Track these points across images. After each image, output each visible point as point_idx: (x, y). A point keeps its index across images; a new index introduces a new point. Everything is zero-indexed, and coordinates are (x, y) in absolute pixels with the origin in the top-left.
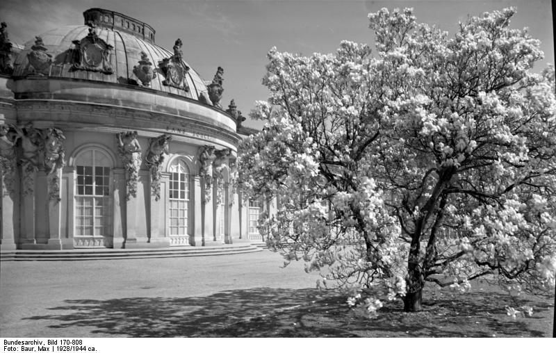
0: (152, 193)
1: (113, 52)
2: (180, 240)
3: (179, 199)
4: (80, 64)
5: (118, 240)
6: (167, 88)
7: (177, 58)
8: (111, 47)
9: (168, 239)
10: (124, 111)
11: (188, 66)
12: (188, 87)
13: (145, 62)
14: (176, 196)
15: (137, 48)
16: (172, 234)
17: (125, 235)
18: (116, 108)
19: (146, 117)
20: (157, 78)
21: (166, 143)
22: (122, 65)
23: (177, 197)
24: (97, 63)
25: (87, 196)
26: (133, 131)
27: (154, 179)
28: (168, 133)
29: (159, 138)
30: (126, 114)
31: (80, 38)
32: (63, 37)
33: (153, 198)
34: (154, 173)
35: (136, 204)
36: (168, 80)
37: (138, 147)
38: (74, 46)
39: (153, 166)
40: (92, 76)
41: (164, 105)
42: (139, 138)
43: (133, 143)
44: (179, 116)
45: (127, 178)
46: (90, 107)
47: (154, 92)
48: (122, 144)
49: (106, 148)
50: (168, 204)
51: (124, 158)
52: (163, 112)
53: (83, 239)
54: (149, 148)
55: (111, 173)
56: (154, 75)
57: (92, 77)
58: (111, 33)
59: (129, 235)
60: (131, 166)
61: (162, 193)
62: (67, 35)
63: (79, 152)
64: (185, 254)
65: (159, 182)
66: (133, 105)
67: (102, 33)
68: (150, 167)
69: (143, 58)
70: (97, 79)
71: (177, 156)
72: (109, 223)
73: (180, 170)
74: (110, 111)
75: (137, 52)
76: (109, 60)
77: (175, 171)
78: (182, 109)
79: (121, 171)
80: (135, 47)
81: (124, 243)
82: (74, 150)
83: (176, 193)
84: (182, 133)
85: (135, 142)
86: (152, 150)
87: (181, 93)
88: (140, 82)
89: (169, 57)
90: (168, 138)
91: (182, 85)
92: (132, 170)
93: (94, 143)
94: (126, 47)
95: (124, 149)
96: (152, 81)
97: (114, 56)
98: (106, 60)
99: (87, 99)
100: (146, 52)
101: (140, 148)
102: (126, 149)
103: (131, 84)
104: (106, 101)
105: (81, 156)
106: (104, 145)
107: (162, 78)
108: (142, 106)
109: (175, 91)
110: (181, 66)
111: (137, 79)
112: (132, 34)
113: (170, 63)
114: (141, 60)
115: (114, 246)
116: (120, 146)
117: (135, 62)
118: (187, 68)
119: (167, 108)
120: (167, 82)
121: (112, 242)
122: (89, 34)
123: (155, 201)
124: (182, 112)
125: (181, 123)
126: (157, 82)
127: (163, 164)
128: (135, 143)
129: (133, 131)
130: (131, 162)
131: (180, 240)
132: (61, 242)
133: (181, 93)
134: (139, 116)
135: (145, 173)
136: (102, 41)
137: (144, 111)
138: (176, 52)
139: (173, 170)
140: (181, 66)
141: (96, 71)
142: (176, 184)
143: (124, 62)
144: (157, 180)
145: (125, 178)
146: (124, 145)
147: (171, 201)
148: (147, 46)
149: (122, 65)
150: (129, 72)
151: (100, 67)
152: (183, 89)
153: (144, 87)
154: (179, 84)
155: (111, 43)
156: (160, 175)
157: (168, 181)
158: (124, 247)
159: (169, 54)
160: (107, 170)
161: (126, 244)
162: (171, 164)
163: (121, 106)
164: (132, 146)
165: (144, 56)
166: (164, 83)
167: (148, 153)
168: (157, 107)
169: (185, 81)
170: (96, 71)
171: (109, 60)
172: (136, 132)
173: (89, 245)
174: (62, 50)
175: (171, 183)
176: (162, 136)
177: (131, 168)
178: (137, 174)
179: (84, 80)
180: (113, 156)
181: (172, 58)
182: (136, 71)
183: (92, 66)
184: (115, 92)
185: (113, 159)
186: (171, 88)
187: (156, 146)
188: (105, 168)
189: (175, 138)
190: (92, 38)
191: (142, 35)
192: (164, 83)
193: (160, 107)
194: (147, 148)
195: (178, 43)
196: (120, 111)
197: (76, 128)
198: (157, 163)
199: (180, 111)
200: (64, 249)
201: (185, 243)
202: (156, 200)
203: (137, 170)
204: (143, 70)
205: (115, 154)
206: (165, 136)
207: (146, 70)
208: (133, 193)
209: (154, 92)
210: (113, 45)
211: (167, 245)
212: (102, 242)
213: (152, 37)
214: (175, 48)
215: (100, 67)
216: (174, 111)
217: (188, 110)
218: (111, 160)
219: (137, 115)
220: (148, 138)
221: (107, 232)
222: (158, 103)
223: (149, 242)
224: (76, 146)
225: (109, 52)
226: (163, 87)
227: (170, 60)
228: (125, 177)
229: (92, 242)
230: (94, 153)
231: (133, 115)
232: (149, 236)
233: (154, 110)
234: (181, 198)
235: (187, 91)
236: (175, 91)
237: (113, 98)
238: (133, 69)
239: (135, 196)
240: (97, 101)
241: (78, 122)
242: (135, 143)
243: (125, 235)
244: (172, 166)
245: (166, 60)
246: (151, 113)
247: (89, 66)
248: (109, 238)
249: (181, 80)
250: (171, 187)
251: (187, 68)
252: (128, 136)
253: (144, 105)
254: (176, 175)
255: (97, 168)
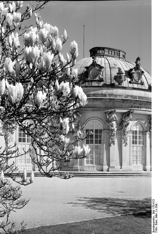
0: (123, 142)
1: (104, 69)
2: (138, 167)
3: (138, 145)
4: (88, 78)
5: (105, 167)
6: (132, 84)
7: (137, 68)
8: (103, 67)
9: (131, 167)
10: (109, 100)
11: (143, 70)
12: (143, 82)
13: (120, 72)
14: (136, 143)
15: (116, 65)
16: (133, 164)
17: (109, 164)
18: (105, 99)
19: (120, 102)
20: (126, 80)
21: (130, 115)
22: (107, 75)
23: (137, 144)
24: (96, 77)
25: (94, 146)
26: (113, 110)
27: (124, 134)
28: (132, 110)
29: (127, 112)
30: (110, 102)
31: (88, 65)
32: (81, 65)
33: (123, 145)
34: (124, 131)
35: (114, 148)
36: (132, 80)
37: (116, 118)
38: (86, 69)
39: (123, 128)
40: (95, 84)
41: (130, 94)
42: (117, 113)
43: (113, 116)
44: (138, 99)
45: (110, 135)
46: (92, 100)
47: (124, 88)
48: (108, 117)
49: (100, 120)
50: (132, 148)
51: (109, 124)
52: (129, 98)
53: (89, 167)
54: (122, 118)
55: (103, 132)
56: (125, 79)
57: (94, 84)
58: (103, 59)
59: (111, 165)
60: (112, 128)
61: (128, 142)
62: (83, 64)
63: (87, 122)
64: (139, 175)
65: (126, 136)
66: (113, 96)
67: (100, 60)
68: (122, 128)
69: (119, 71)
70: (96, 85)
71: (136, 122)
72: (101, 158)
73: (137, 129)
74: (102, 101)
75: (116, 67)
76: (102, 74)
77: (135, 130)
78: (140, 95)
79: (107, 131)
80: (115, 65)
81: (108, 169)
82: (85, 121)
83: (136, 142)
84: (139, 109)
85: (114, 115)
86: (123, 119)
87: (140, 86)
88: (117, 84)
89: (133, 67)
90: (132, 112)
91: (140, 82)
92: (113, 130)
93: (94, 117)
94: (111, 66)
95: (109, 120)
96: (124, 82)
97: (104, 72)
98: (101, 74)
99: (91, 96)
100: (121, 67)
101: (117, 119)
102: (110, 120)
103: (112, 86)
104: (100, 96)
105: (88, 124)
106: (99, 118)
107: (129, 80)
108: (118, 96)
109: (136, 86)
110: (140, 72)
111: (117, 81)
112: (114, 57)
113: (133, 71)
114: (118, 72)
115: (104, 170)
116: (107, 118)
117: (115, 73)
118: (143, 72)
119: (131, 96)
120: (132, 81)
121: (103, 168)
122: (93, 63)
123: (124, 147)
124: (140, 97)
125: (139, 104)
126: (125, 84)
127: (129, 126)
128: (115, 116)
129: (113, 110)
130: (112, 126)
131: (138, 167)
132: (79, 167)
133: (140, 86)
134: (117, 102)
135: (120, 131)
136: (99, 65)
137: (119, 99)
138: (136, 64)
139: (134, 129)
140: (140, 72)
141: (95, 81)
142: (136, 137)
143: (110, 74)
144: (126, 135)
145: (109, 135)
146: (109, 117)
147: (133, 146)
148: (121, 63)
149: (107, 75)
150: (112, 79)
151: (97, 78)
152: (140, 84)
153: (119, 86)
154: (138, 82)
155: (103, 65)
156: (127, 132)
157: (131, 135)
158: (108, 171)
159: (133, 66)
160: (101, 131)
161: (110, 169)
162: (133, 126)
163: (108, 98)
164: (113, 117)
165: (120, 69)
166: (130, 82)
167: (121, 121)
168: (126, 96)
169: (142, 79)
170: (95, 81)
171: (102, 74)
172: (115, 111)
173: (91, 170)
174: (80, 72)
175: (133, 136)
176: (129, 111)
177: (112, 129)
178: (115, 133)
179: (90, 87)
180: (103, 123)
181: (134, 68)
182: (116, 78)
183: (94, 78)
184: (104, 91)
185: (103, 125)
186: (134, 84)
187: (125, 117)
188: (100, 130)
189: (135, 112)
190: (94, 64)
191: (119, 57)
192: (130, 82)
193: (127, 96)
194: (121, 118)
195: (138, 59)
196: (107, 100)
197: (86, 110)
198: (126, 126)
199: (138, 96)
200: (80, 171)
201: (140, 169)
202: (125, 146)
203: (115, 130)
204: (118, 78)
205: (104, 123)
206: (130, 111)
207: (120, 77)
208: (113, 142)
209: (124, 88)
210: (104, 66)
211: (131, 170)
212: (95, 168)
213: (124, 56)
214: (136, 62)
215: (97, 78)
216: (135, 97)
217: (143, 96)
218: (102, 125)
219: (115, 102)
220: (121, 113)
221: (100, 163)
222: (127, 94)
223: (121, 168)
224: (86, 120)
225: (102, 70)
226: (129, 84)
227: (134, 69)
228: (109, 134)
229: (93, 168)
230: (94, 122)
231: (113, 101)
232: (121, 164)
233: (124, 97)
234: (139, 144)
235: (142, 85)
236: (136, 86)
237: (104, 94)
238: (114, 77)
239: (114, 144)
240: (96, 96)
241: (87, 108)
242: (115, 116)
243: (109, 164)
244: (134, 127)
245: (131, 70)
246: (123, 100)
247: (93, 79)
248: (101, 166)
249: (139, 80)
250: (133, 138)
251: (143, 72)
252: (111, 113)
253: (119, 95)
254: (136, 132)
255: (95, 130)
